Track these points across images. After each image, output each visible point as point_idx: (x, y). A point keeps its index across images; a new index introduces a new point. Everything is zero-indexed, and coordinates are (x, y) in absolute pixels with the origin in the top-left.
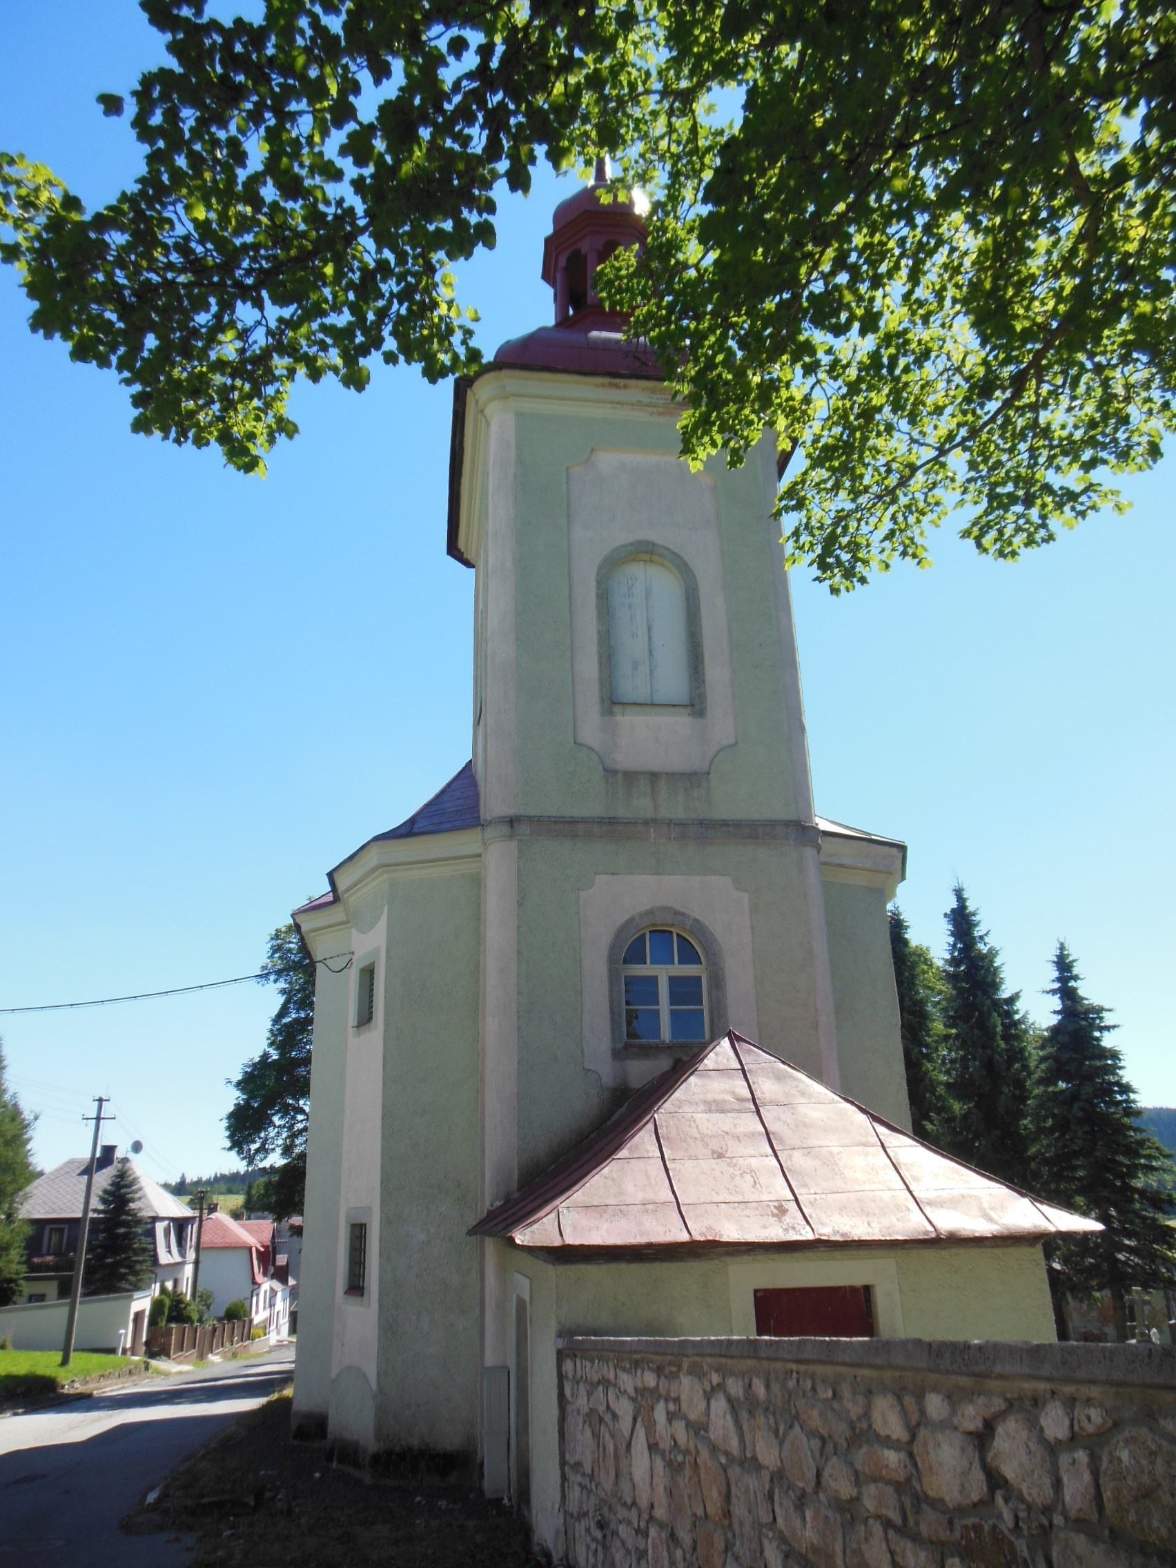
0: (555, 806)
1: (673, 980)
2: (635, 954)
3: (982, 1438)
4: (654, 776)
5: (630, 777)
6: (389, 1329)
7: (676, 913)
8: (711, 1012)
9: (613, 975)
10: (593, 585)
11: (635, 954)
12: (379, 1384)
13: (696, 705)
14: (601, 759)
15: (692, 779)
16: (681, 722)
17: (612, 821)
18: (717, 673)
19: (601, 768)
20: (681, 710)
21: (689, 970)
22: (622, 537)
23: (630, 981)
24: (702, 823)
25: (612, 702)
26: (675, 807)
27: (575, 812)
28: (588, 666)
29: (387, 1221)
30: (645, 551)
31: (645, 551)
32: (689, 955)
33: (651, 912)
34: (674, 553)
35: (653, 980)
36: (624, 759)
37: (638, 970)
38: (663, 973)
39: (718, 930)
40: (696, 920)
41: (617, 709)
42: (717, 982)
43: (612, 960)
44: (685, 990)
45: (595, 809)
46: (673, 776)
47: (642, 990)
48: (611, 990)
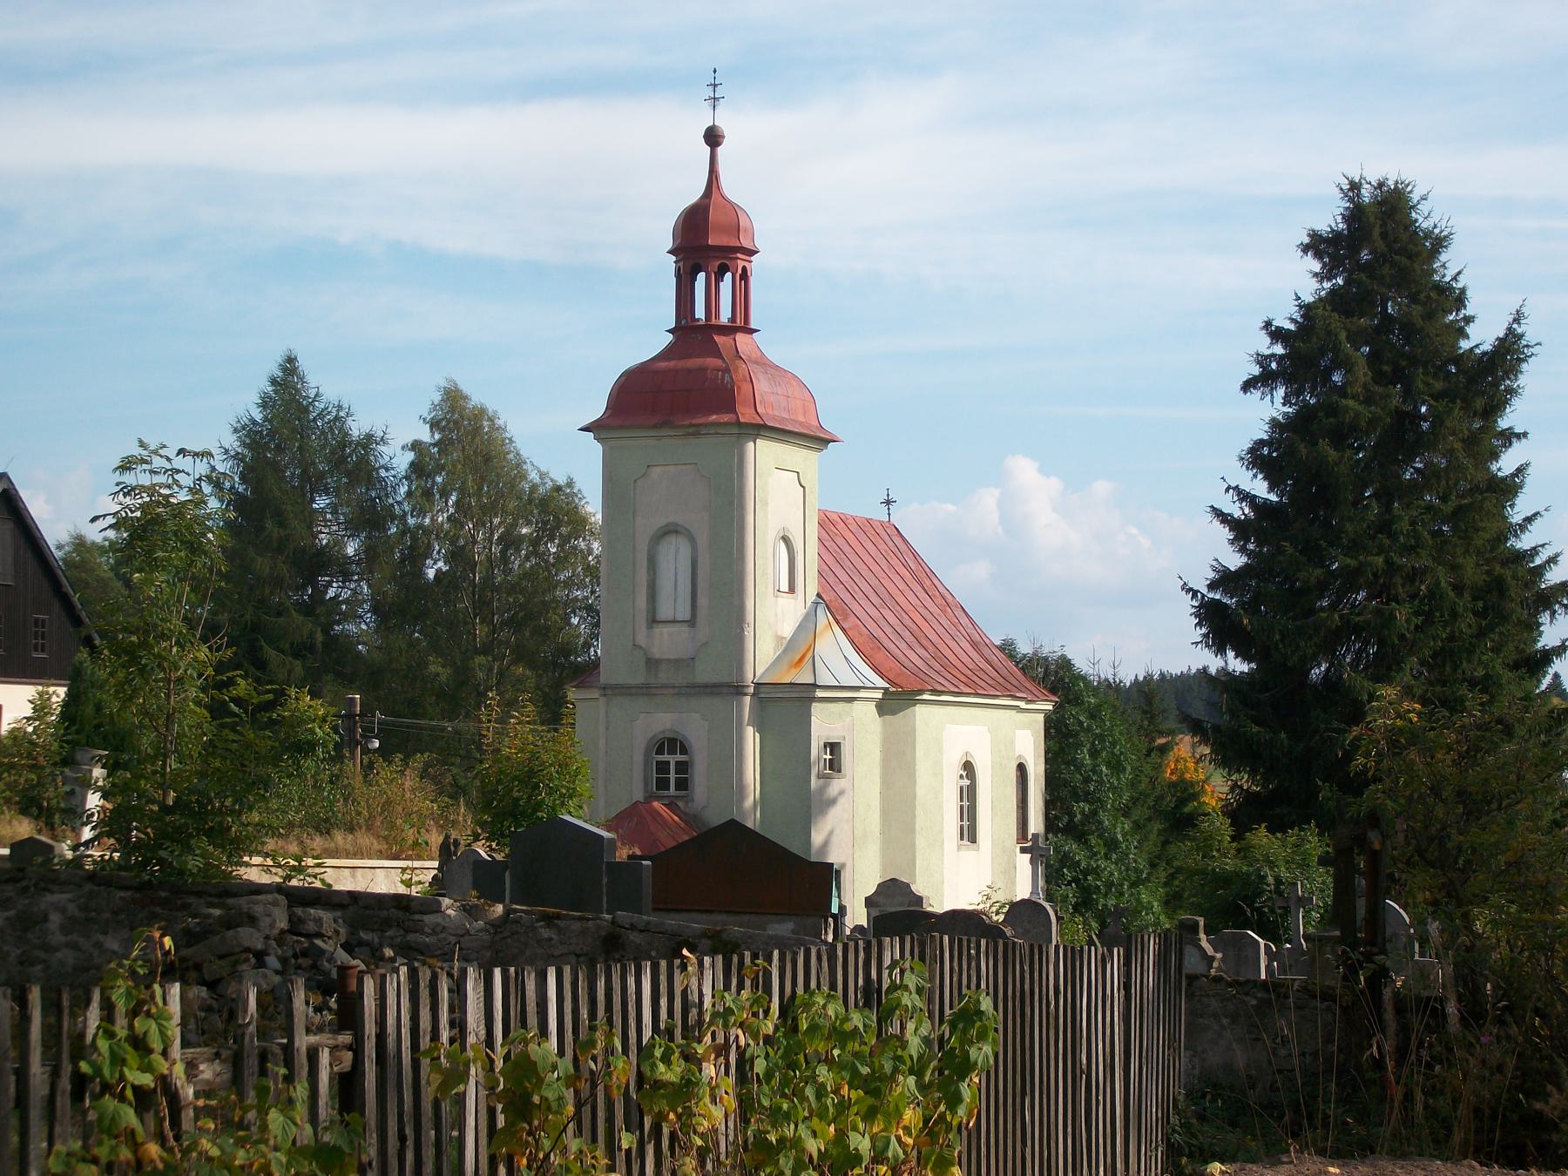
2: (660, 751)
4: (668, 660)
7: (676, 732)
9: (646, 763)
13: (692, 622)
16: (685, 628)
17: (647, 686)
18: (702, 601)
20: (686, 624)
21: (683, 758)
22: (660, 521)
25: (653, 621)
27: (632, 682)
28: (642, 602)
30: (670, 530)
31: (670, 530)
33: (663, 732)
36: (657, 653)
37: (661, 758)
38: (672, 759)
39: (693, 741)
41: (655, 625)
43: (647, 754)
44: (683, 767)
45: (640, 680)
47: (663, 767)
48: (645, 770)
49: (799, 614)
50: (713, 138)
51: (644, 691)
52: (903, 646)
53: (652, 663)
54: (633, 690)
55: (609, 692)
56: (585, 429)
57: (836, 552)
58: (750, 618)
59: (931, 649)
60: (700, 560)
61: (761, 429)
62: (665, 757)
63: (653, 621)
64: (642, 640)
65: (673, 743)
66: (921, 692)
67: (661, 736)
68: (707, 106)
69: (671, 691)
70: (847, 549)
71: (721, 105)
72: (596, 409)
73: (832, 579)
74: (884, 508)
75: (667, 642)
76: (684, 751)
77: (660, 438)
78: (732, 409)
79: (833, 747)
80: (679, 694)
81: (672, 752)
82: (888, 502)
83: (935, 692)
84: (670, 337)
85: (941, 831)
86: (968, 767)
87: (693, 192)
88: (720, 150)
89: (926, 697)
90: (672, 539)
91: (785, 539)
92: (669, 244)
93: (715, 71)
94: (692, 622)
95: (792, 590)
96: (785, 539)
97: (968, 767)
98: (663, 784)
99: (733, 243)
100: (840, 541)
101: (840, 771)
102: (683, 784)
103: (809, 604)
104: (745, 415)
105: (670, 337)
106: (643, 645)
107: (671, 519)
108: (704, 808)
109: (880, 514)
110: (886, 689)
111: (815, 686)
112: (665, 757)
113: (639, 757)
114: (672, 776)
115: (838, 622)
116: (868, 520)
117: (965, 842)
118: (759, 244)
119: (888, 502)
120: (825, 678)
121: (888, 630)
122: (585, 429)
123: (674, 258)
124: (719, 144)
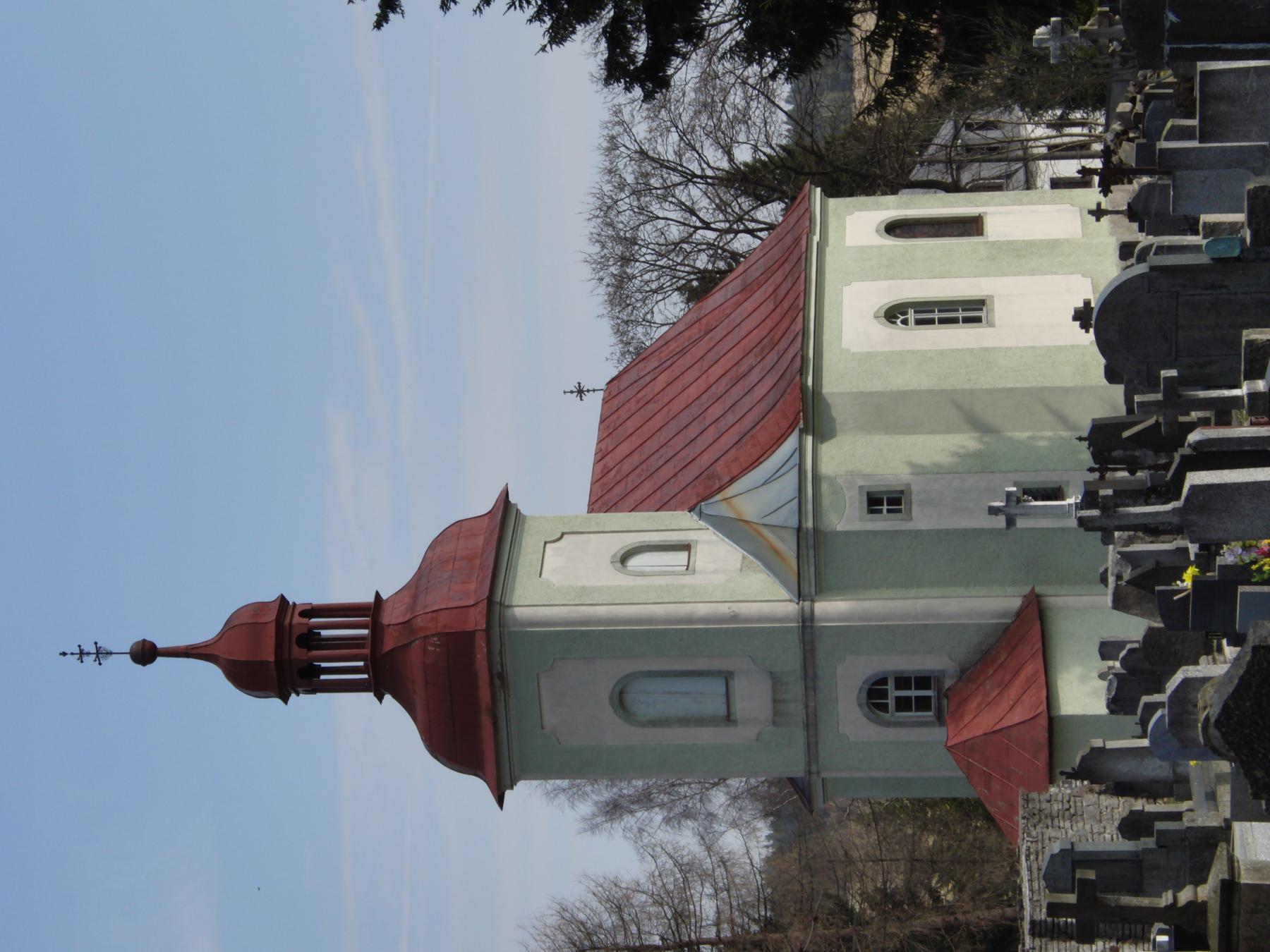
1: (898, 687)
2: (884, 708)
4: (775, 701)
5: (776, 713)
11: (884, 708)
13: (727, 676)
15: (776, 681)
17: (808, 726)
18: (701, 664)
20: (731, 682)
22: (608, 714)
24: (805, 677)
25: (729, 719)
26: (796, 690)
28: (705, 736)
30: (620, 701)
33: (860, 706)
34: (617, 683)
35: (898, 699)
38: (893, 693)
40: (864, 683)
41: (732, 717)
43: (888, 724)
44: (903, 681)
45: (799, 735)
46: (774, 691)
49: (714, 537)
50: (145, 654)
51: (811, 725)
52: (749, 401)
55: (814, 769)
56: (500, 801)
57: (639, 476)
58: (724, 609)
59: (751, 360)
61: (493, 604)
62: (891, 702)
63: (729, 719)
65: (875, 695)
66: (803, 387)
67: (866, 709)
68: (108, 662)
70: (636, 459)
71: (106, 644)
72: (475, 788)
73: (671, 489)
74: (588, 397)
76: (883, 681)
78: (472, 634)
79: (874, 502)
81: (884, 694)
82: (580, 392)
83: (802, 371)
84: (388, 698)
85: (971, 351)
86: (893, 314)
87: (211, 674)
89: (810, 382)
90: (628, 698)
91: (624, 558)
92: (277, 702)
93: (64, 654)
95: (686, 547)
96: (624, 558)
97: (893, 314)
98: (923, 704)
99: (271, 631)
100: (627, 466)
101: (902, 492)
102: (923, 681)
103: (702, 523)
104: (476, 620)
105: (388, 698)
108: (950, 658)
109: (594, 402)
110: (801, 432)
111: (799, 529)
112: (891, 702)
113: (891, 734)
114: (913, 693)
115: (721, 489)
116: (602, 422)
117: (983, 314)
118: (270, 596)
119: (580, 392)
120: (787, 516)
121: (730, 419)
122: (500, 801)
123: (293, 696)
124: (153, 646)
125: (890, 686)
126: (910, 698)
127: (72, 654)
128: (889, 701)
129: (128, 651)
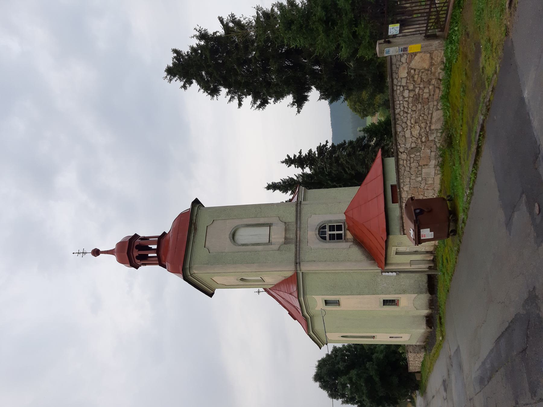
0: (292, 255)
3: (401, 153)
6: (404, 292)
8: (337, 223)
9: (329, 242)
10: (240, 247)
11: (324, 238)
12: (416, 294)
13: (270, 225)
14: (282, 245)
18: (262, 221)
19: (284, 245)
21: (327, 228)
22: (228, 241)
23: (330, 239)
27: (294, 250)
28: (260, 248)
29: (382, 293)
31: (233, 236)
32: (324, 227)
35: (330, 235)
39: (320, 221)
42: (330, 221)
43: (326, 242)
44: (332, 228)
45: (293, 246)
50: (96, 252)
53: (287, 241)
54: (298, 249)
55: (298, 261)
60: (245, 223)
62: (327, 236)
64: (276, 247)
65: (321, 232)
69: (298, 232)
71: (86, 250)
75: (278, 236)
76: (324, 227)
77: (193, 242)
80: (300, 228)
81: (325, 233)
87: (113, 258)
88: (101, 250)
93: (74, 253)
94: (270, 225)
98: (339, 237)
102: (339, 228)
106: (279, 246)
107: (228, 236)
112: (327, 236)
114: (336, 232)
125: (327, 229)
126: (334, 234)
127: (76, 253)
128: (327, 236)
129: (91, 252)
